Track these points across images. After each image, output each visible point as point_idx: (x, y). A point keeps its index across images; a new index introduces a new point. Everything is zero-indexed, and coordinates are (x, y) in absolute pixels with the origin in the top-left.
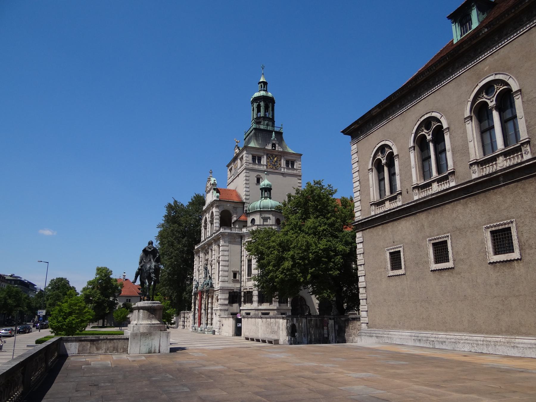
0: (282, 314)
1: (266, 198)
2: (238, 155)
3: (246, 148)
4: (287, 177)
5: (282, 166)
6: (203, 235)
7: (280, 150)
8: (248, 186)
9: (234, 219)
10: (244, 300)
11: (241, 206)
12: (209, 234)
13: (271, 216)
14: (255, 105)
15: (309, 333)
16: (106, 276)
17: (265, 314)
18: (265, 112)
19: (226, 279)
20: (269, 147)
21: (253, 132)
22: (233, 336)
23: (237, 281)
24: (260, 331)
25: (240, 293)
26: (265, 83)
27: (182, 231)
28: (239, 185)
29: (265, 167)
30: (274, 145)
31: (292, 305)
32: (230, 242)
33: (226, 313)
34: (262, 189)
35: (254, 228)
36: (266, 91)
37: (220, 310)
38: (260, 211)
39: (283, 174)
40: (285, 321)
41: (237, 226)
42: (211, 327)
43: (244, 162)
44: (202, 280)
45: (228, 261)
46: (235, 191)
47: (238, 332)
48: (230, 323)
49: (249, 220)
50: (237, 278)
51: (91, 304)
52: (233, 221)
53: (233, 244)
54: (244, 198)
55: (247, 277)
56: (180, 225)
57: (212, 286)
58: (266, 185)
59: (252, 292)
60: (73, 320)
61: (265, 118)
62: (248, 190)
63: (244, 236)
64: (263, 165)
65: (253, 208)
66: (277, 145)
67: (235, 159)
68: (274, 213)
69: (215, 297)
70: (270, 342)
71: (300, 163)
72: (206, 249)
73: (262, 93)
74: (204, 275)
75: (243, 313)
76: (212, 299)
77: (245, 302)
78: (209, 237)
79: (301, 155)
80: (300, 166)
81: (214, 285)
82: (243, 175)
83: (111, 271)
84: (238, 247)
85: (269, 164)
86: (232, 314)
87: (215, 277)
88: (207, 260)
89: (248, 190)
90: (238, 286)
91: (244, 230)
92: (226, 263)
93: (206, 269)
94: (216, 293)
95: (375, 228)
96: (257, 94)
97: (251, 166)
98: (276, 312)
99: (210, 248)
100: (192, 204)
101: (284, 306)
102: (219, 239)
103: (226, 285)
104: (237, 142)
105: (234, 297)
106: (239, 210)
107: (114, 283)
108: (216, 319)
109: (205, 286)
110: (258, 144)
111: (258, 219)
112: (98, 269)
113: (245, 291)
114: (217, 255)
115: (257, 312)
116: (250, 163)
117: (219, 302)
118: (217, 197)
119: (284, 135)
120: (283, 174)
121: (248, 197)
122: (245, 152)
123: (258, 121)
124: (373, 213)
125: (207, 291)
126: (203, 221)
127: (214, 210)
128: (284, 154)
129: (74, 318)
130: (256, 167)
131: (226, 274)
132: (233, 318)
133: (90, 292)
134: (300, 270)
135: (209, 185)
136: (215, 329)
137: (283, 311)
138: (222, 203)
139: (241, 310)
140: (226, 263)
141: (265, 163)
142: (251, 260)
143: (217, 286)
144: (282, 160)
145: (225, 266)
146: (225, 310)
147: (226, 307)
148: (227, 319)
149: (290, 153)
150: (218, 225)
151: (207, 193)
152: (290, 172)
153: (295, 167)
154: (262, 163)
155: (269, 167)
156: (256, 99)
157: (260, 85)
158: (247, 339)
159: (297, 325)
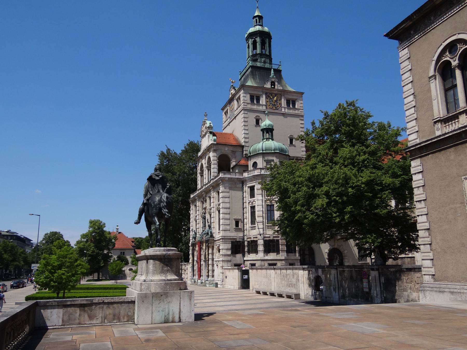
0: (291, 264)
1: (268, 139)
2: (234, 96)
3: (243, 86)
4: (289, 118)
5: (283, 106)
6: (199, 182)
7: (279, 88)
8: (246, 128)
9: (233, 164)
10: (248, 250)
12: (206, 181)
13: (274, 158)
14: (251, 41)
15: (340, 286)
16: (99, 228)
17: (272, 265)
19: (228, 227)
20: (268, 85)
21: (249, 70)
22: (239, 289)
23: (240, 230)
24: (273, 283)
25: (243, 242)
26: (260, 17)
27: (175, 180)
28: (237, 128)
29: (264, 108)
30: (273, 84)
31: (300, 255)
32: (231, 188)
33: (229, 264)
34: (263, 130)
35: (257, 172)
36: (262, 25)
37: (223, 261)
38: (263, 154)
39: (284, 115)
40: (307, 272)
41: (237, 171)
42: (212, 279)
43: (241, 102)
44: (200, 231)
45: (229, 208)
46: (231, 134)
47: (245, 284)
48: (234, 277)
49: (250, 163)
50: (240, 227)
51: (86, 257)
52: (232, 166)
53: (234, 190)
54: (242, 141)
55: (250, 226)
56: (174, 174)
57: (212, 236)
58: (267, 125)
59: (257, 241)
60: (63, 274)
61: (261, 55)
62: (246, 132)
63: (246, 181)
64: (262, 105)
65: (255, 150)
66: (276, 83)
67: (231, 100)
68: (278, 155)
69: (216, 247)
70: (289, 297)
71: (302, 102)
72: (204, 197)
73: (258, 28)
74: (201, 225)
75: (248, 263)
76: (213, 250)
77: (249, 252)
78: (207, 184)
79: (302, 93)
80: (302, 105)
81: (214, 235)
82: (241, 116)
83: (105, 224)
84: (240, 193)
85: (268, 103)
86: (235, 265)
87: (215, 225)
88: (205, 209)
89: (246, 132)
90: (241, 234)
91: (246, 175)
92: (228, 211)
93: (204, 218)
94: (217, 243)
95: (443, 152)
96: (252, 30)
97: (249, 106)
98: (284, 262)
99: (208, 195)
100: (185, 152)
101: (292, 256)
102: (218, 185)
103: (228, 234)
104: (232, 82)
105: (237, 247)
106: (238, 154)
107: (108, 236)
108: (218, 271)
109: (205, 236)
110: (256, 83)
111: (260, 162)
112: (91, 222)
113: (249, 240)
114: (216, 202)
115: (263, 263)
116: (249, 104)
117: (221, 253)
118: (214, 140)
119: (283, 73)
120: (284, 115)
121: (247, 140)
122: (242, 91)
123: (254, 58)
124: (438, 133)
125: (207, 241)
126: (199, 168)
127: (211, 154)
128: (284, 92)
129: (64, 272)
130: (255, 107)
131: (228, 222)
132: (238, 269)
133: (84, 245)
134: (338, 209)
135: (204, 128)
136: (217, 282)
137: (291, 262)
138: (220, 147)
139: (244, 261)
140: (228, 211)
141: (264, 103)
142: (255, 206)
143: (217, 236)
144: (283, 100)
145: (226, 214)
146: (228, 261)
147: (229, 258)
148: (231, 271)
149: (290, 92)
150: (216, 170)
151: (203, 138)
152: (291, 112)
153: (296, 107)
155: (268, 107)
156: (252, 35)
157: (255, 19)
158: (258, 292)
159: (323, 277)
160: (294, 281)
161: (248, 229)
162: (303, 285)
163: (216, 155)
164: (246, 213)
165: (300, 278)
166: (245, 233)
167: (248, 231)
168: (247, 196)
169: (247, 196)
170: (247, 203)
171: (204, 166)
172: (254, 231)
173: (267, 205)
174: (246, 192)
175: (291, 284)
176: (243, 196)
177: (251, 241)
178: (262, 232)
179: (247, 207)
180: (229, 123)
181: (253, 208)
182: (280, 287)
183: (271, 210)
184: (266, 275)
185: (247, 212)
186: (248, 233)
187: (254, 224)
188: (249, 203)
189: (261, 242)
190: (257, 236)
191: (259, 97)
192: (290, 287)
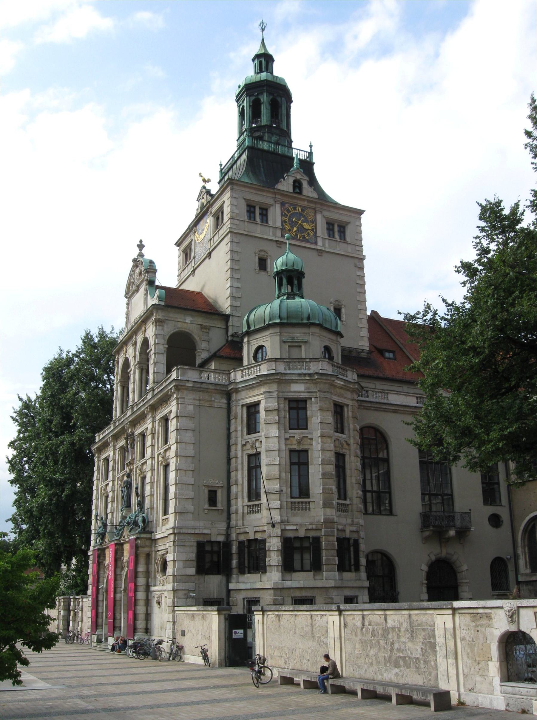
5: (319, 234)
11: (221, 324)
17: (303, 601)
18: (272, 116)
25: (227, 544)
34: (279, 274)
43: (226, 218)
48: (204, 630)
52: (198, 362)
55: (246, 502)
58: (290, 264)
59: (264, 541)
66: (305, 184)
79: (361, 212)
91: (238, 376)
113: (242, 538)
118: (160, 298)
120: (320, 252)
137: (349, 593)
141: (279, 224)
142: (258, 454)
153: (348, 239)
154: (270, 222)
157: (256, 62)
160: (415, 648)
161: (240, 511)
162: (451, 661)
164: (237, 470)
165: (440, 640)
166: (233, 523)
167: (240, 515)
168: (239, 428)
169: (239, 428)
170: (239, 447)
171: (132, 363)
172: (258, 515)
173: (291, 451)
174: (236, 418)
175: (404, 658)
176: (229, 429)
177: (249, 541)
178: (277, 518)
179: (240, 454)
180: (194, 271)
181: (254, 459)
182: (359, 667)
183: (299, 464)
184: (308, 629)
185: (240, 467)
186: (240, 523)
187: (258, 496)
188: (243, 446)
189: (274, 544)
190: (265, 528)
191: (266, 210)
192: (397, 665)
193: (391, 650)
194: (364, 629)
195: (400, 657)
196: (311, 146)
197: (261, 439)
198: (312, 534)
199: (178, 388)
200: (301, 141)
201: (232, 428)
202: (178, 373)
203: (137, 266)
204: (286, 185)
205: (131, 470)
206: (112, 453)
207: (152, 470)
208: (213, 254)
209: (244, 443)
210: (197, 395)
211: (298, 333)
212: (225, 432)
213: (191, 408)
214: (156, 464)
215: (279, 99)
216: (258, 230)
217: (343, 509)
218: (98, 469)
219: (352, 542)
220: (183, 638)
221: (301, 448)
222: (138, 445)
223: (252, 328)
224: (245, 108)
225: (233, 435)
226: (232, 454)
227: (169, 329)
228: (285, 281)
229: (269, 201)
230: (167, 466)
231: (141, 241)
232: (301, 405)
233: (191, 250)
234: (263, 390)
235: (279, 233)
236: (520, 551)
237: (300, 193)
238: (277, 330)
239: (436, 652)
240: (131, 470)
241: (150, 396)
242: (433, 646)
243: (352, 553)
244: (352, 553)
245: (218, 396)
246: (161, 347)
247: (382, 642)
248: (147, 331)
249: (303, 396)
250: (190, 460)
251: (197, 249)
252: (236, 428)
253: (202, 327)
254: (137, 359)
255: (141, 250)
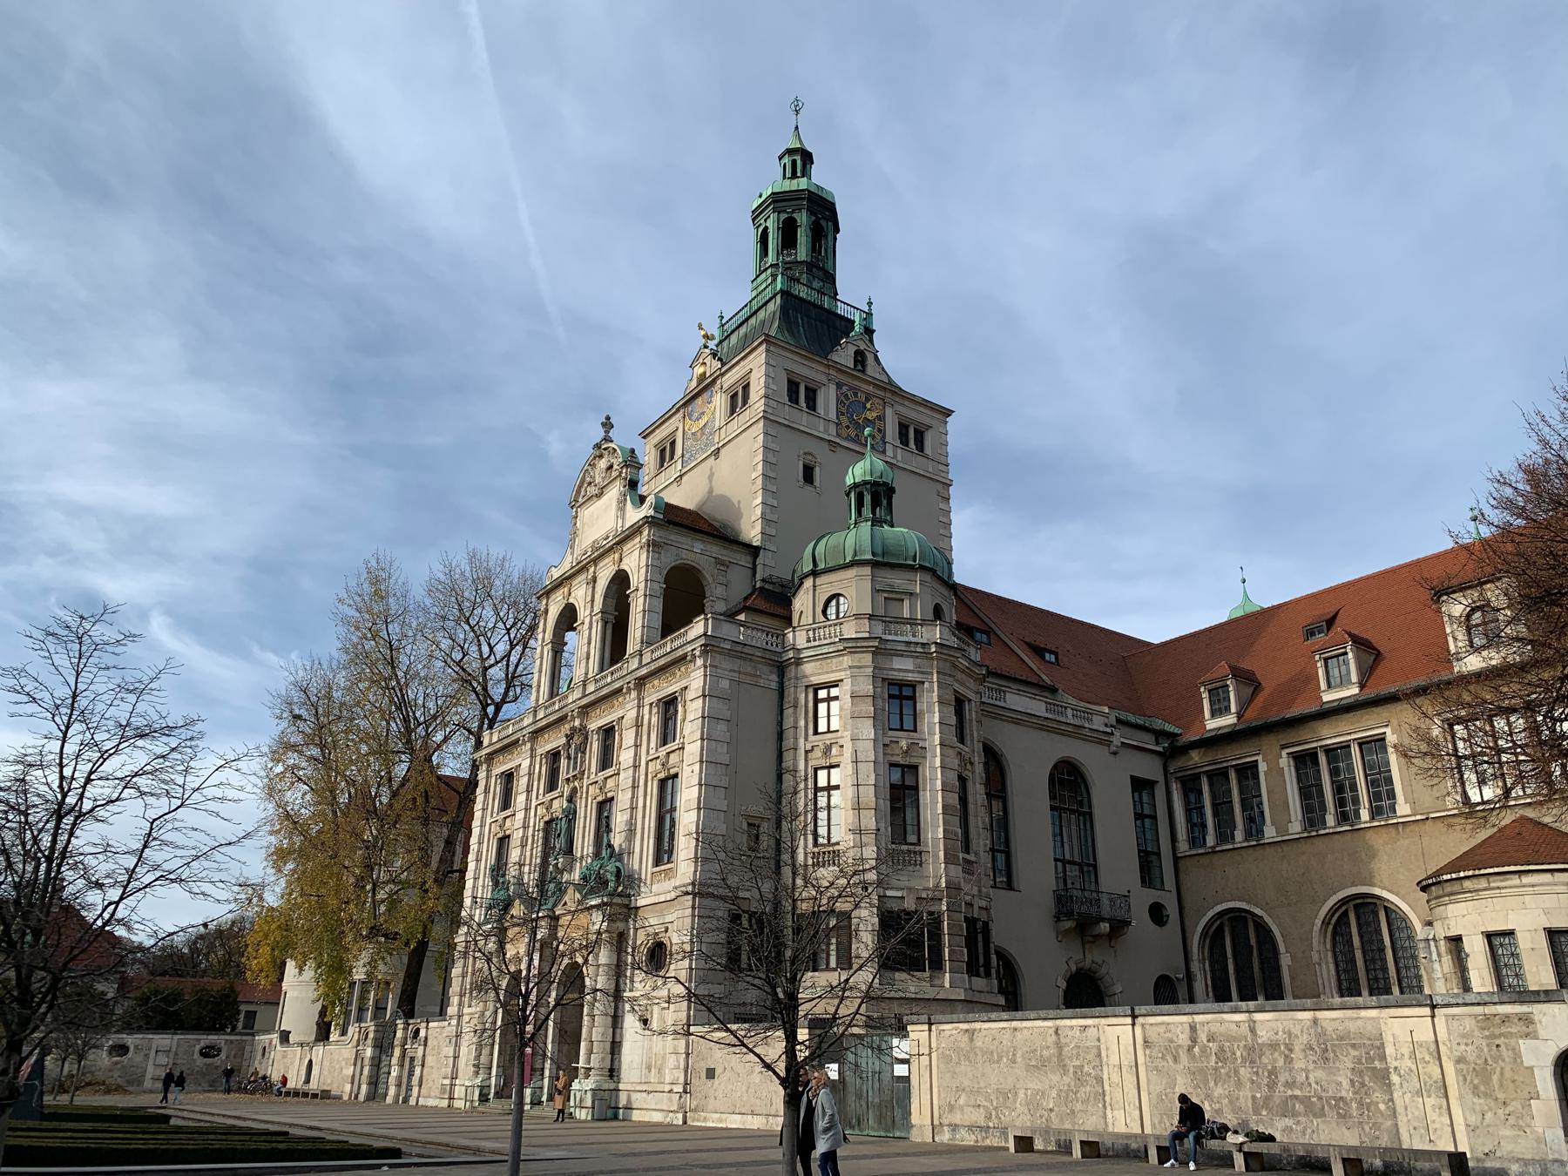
11: (745, 560)
21: (771, 307)
54: (752, 532)
79: (948, 413)
141: (833, 416)
153: (928, 450)
154: (820, 410)
157: (786, 160)
163: (657, 563)
168: (802, 723)
171: (583, 614)
173: (892, 765)
175: (1305, 1100)
176: (781, 724)
189: (866, 921)
193: (1272, 1086)
194: (1196, 1049)
195: (1296, 1097)
196: (870, 304)
197: (841, 742)
198: (925, 908)
199: (707, 649)
200: (851, 291)
201: (788, 723)
202: (706, 626)
203: (601, 456)
204: (844, 355)
205: (574, 790)
206: (526, 764)
207: (634, 787)
208: (723, 451)
209: (809, 747)
210: (737, 664)
211: (898, 580)
212: (773, 728)
213: (725, 684)
214: (642, 778)
215: (823, 223)
216: (803, 420)
217: (968, 867)
218: (486, 791)
219: (980, 925)
220: (709, 1083)
221: (907, 761)
222: (595, 746)
223: (821, 566)
224: (770, 230)
225: (788, 734)
226: (788, 762)
227: (669, 560)
228: (867, 499)
229: (822, 378)
230: (667, 784)
231: (608, 418)
232: (907, 692)
233: (673, 443)
234: (847, 660)
235: (833, 429)
236: (1195, 967)
237: (863, 371)
238: (867, 570)
239: (1390, 1085)
240: (574, 790)
241: (634, 664)
242: (1383, 1077)
243: (980, 944)
244: (980, 944)
245: (766, 669)
246: (656, 586)
247: (1245, 1072)
248: (625, 561)
249: (911, 677)
250: (721, 770)
251: (688, 443)
252: (796, 722)
253: (718, 562)
254: (598, 606)
255: (607, 432)
